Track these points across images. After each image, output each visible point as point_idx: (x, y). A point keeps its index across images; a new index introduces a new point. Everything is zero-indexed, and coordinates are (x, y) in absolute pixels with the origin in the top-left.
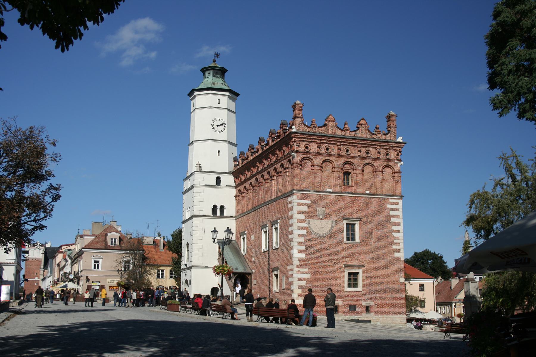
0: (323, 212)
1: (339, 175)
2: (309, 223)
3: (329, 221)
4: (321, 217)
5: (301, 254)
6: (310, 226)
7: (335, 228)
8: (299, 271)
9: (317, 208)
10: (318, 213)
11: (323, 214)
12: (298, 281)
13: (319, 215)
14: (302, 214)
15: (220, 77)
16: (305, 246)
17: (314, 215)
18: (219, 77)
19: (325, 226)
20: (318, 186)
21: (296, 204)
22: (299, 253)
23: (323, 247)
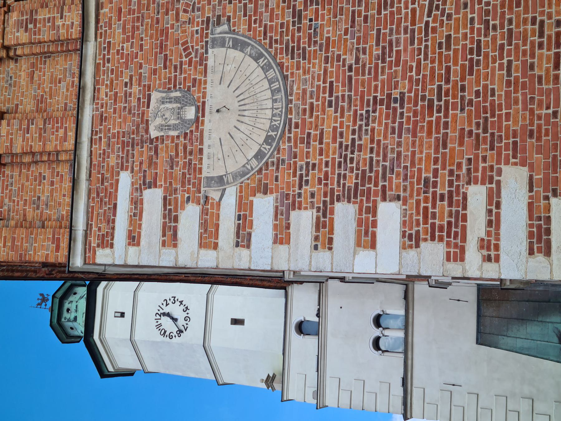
0: (170, 100)
1: (19, 24)
2: (220, 180)
3: (210, 63)
4: (193, 108)
5: (379, 231)
6: (236, 176)
7: (243, 27)
8: (483, 244)
9: (154, 133)
10: (175, 127)
11: (177, 100)
12: (548, 252)
13: (184, 121)
14: (176, 219)
15: (77, 302)
16: (338, 206)
17: (181, 154)
18: (77, 306)
19: (233, 87)
20: (61, 132)
21: (132, 250)
22: (373, 246)
23: (340, 90)
